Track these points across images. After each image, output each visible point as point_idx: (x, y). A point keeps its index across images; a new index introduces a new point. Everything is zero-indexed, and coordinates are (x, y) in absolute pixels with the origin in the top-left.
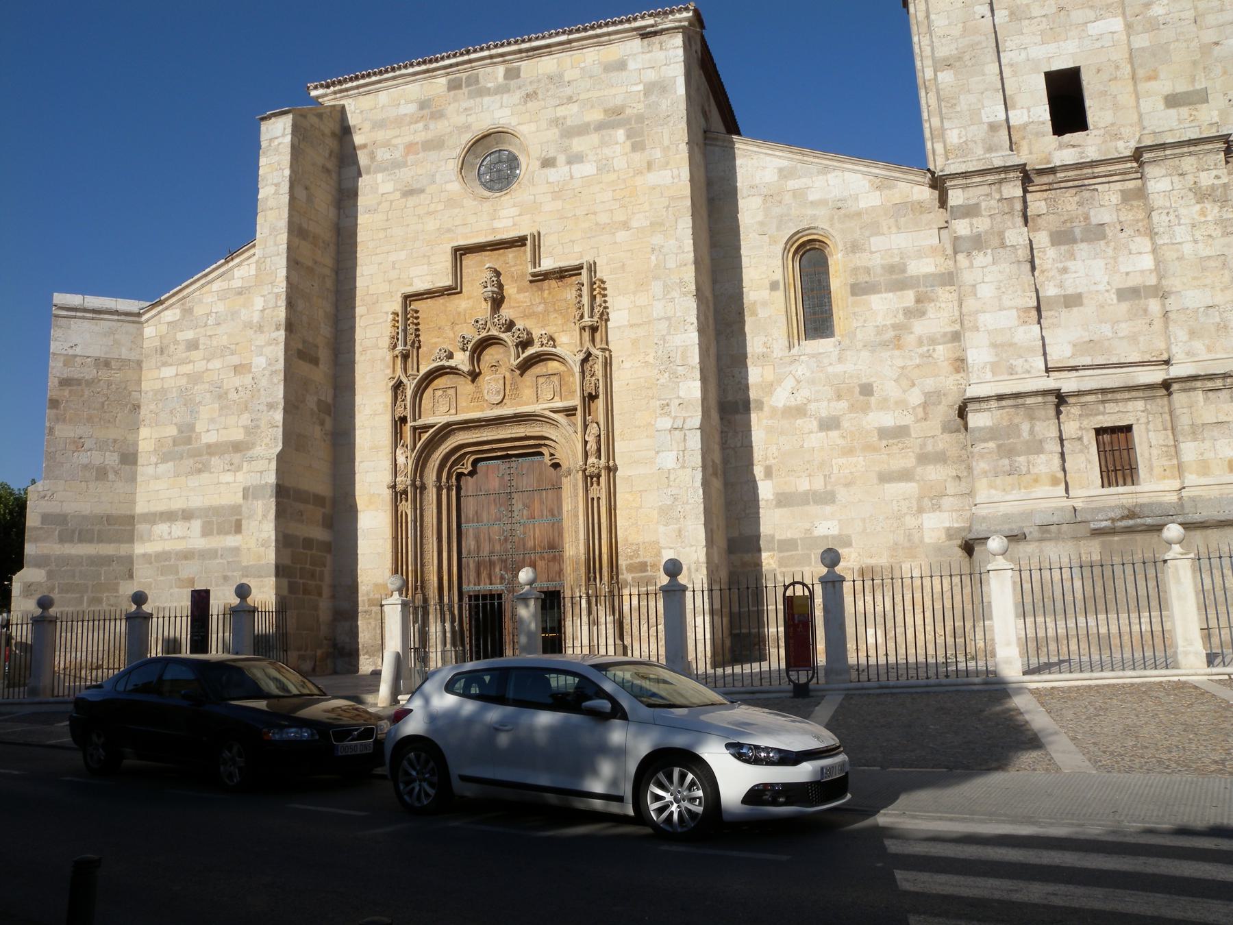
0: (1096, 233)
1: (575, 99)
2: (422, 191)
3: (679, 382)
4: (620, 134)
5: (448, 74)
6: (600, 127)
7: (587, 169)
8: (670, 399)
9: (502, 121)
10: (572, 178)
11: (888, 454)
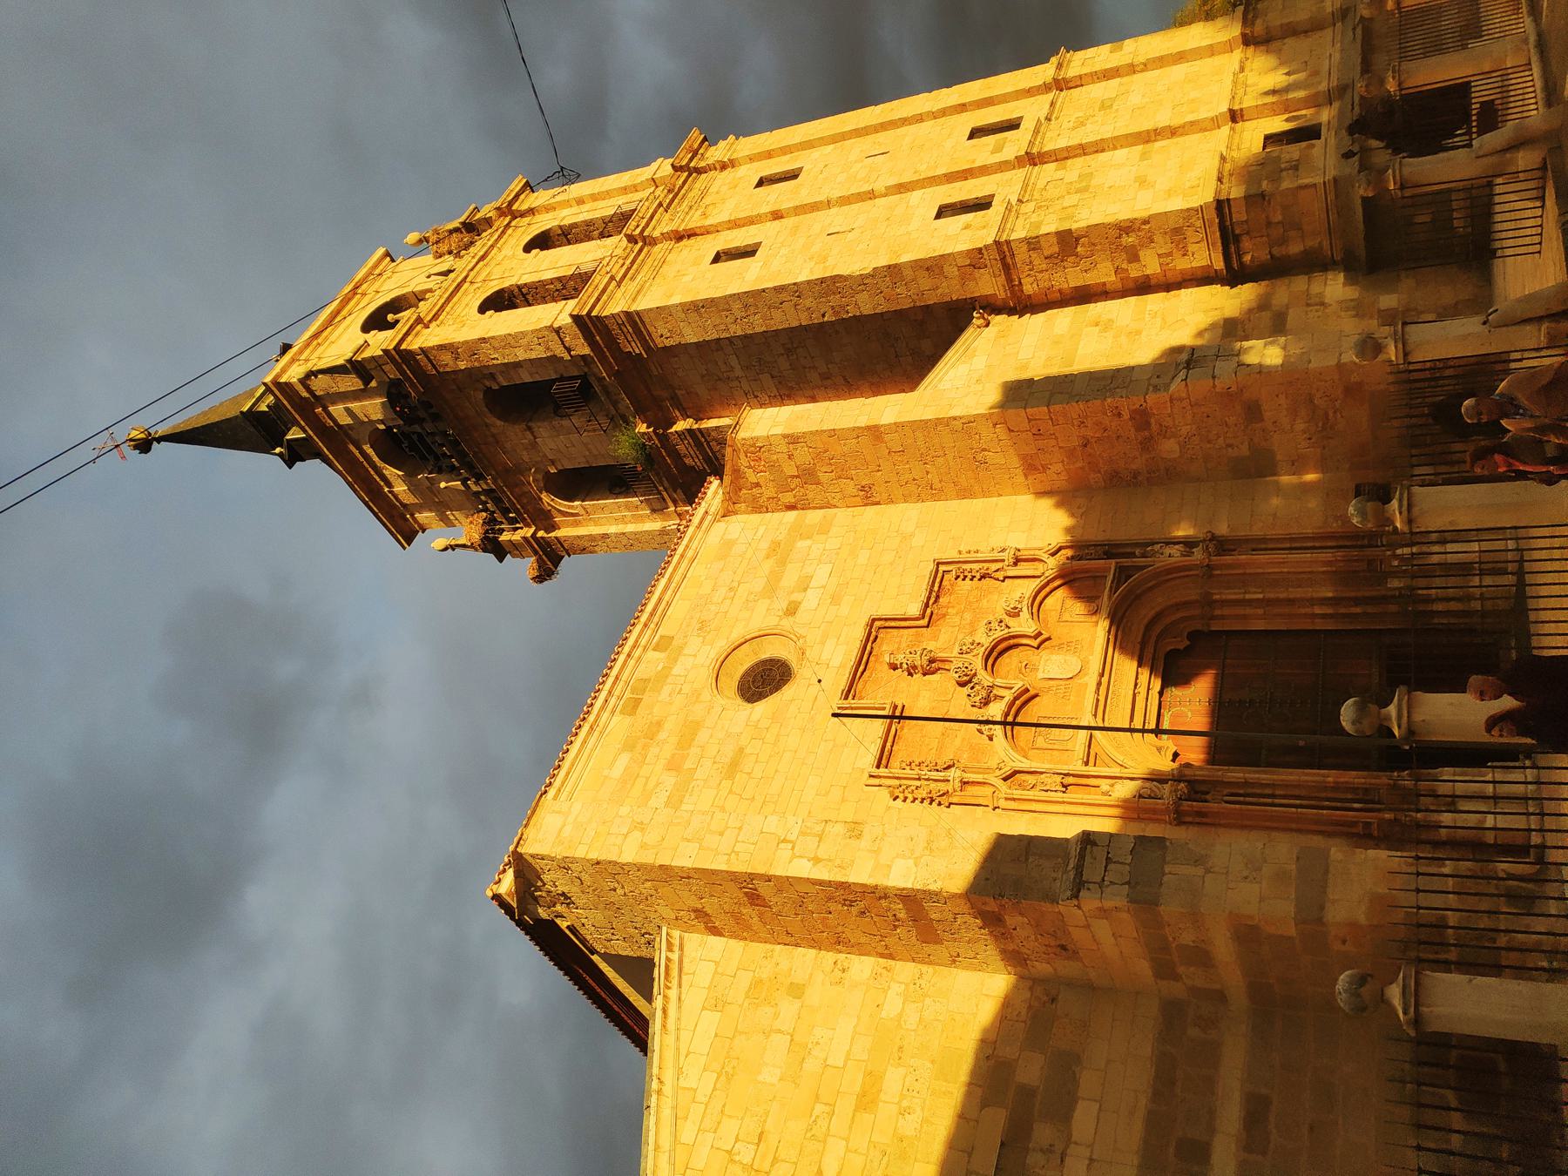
0: (1086, 176)
1: (735, 584)
2: (741, 750)
3: (1131, 381)
4: (802, 544)
5: (613, 712)
6: (782, 563)
7: (821, 574)
8: (1149, 385)
9: (713, 654)
10: (824, 587)
11: (1253, 330)
